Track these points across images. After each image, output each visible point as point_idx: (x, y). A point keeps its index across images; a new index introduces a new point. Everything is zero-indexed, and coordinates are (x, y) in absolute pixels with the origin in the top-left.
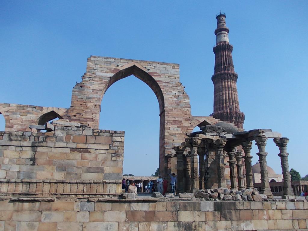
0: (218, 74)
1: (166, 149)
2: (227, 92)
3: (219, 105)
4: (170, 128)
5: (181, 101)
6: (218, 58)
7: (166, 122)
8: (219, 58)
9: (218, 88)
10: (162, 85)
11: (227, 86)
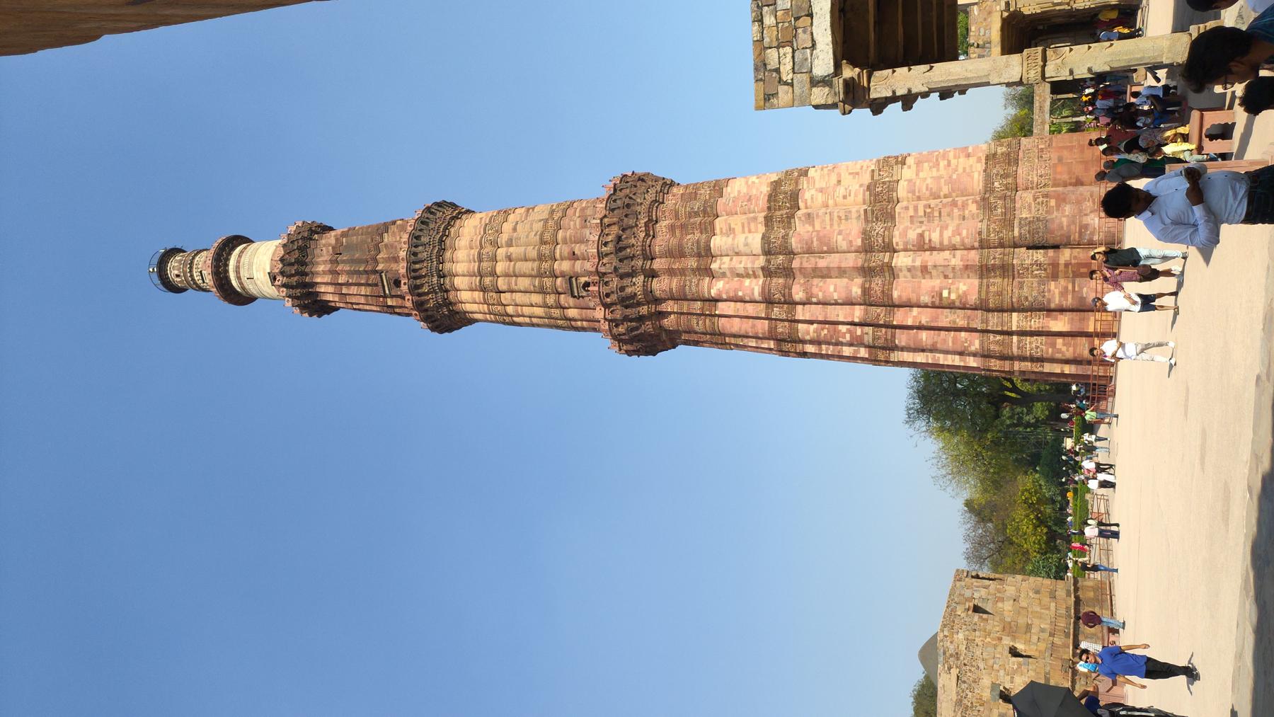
2: (506, 298)
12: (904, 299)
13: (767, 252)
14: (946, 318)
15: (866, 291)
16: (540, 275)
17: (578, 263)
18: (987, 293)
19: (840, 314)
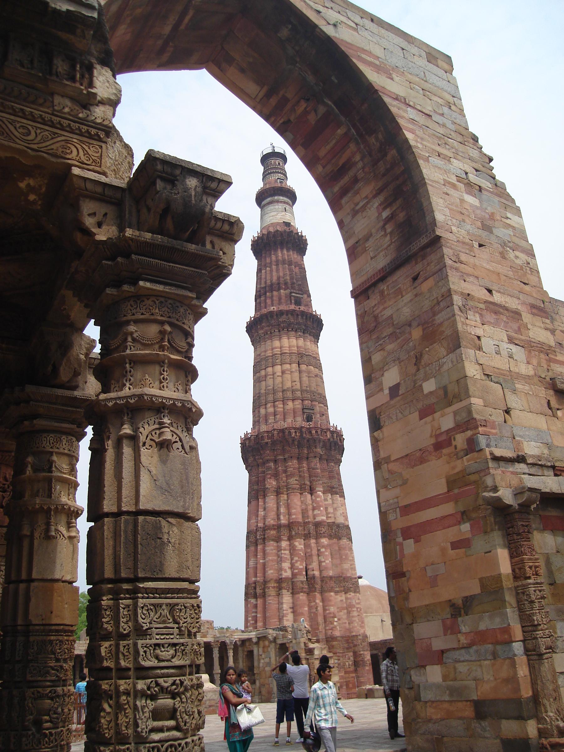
0: (271, 312)
1: (496, 459)
3: (274, 406)
4: (479, 338)
5: (493, 214)
6: (268, 269)
7: (460, 304)
8: (270, 267)
9: (269, 353)
10: (405, 115)
11: (296, 348)
12: (331, 598)
13: (338, 526)
14: (320, 619)
15: (331, 578)
16: (313, 392)
17: (318, 416)
18: (339, 641)
19: (315, 565)
